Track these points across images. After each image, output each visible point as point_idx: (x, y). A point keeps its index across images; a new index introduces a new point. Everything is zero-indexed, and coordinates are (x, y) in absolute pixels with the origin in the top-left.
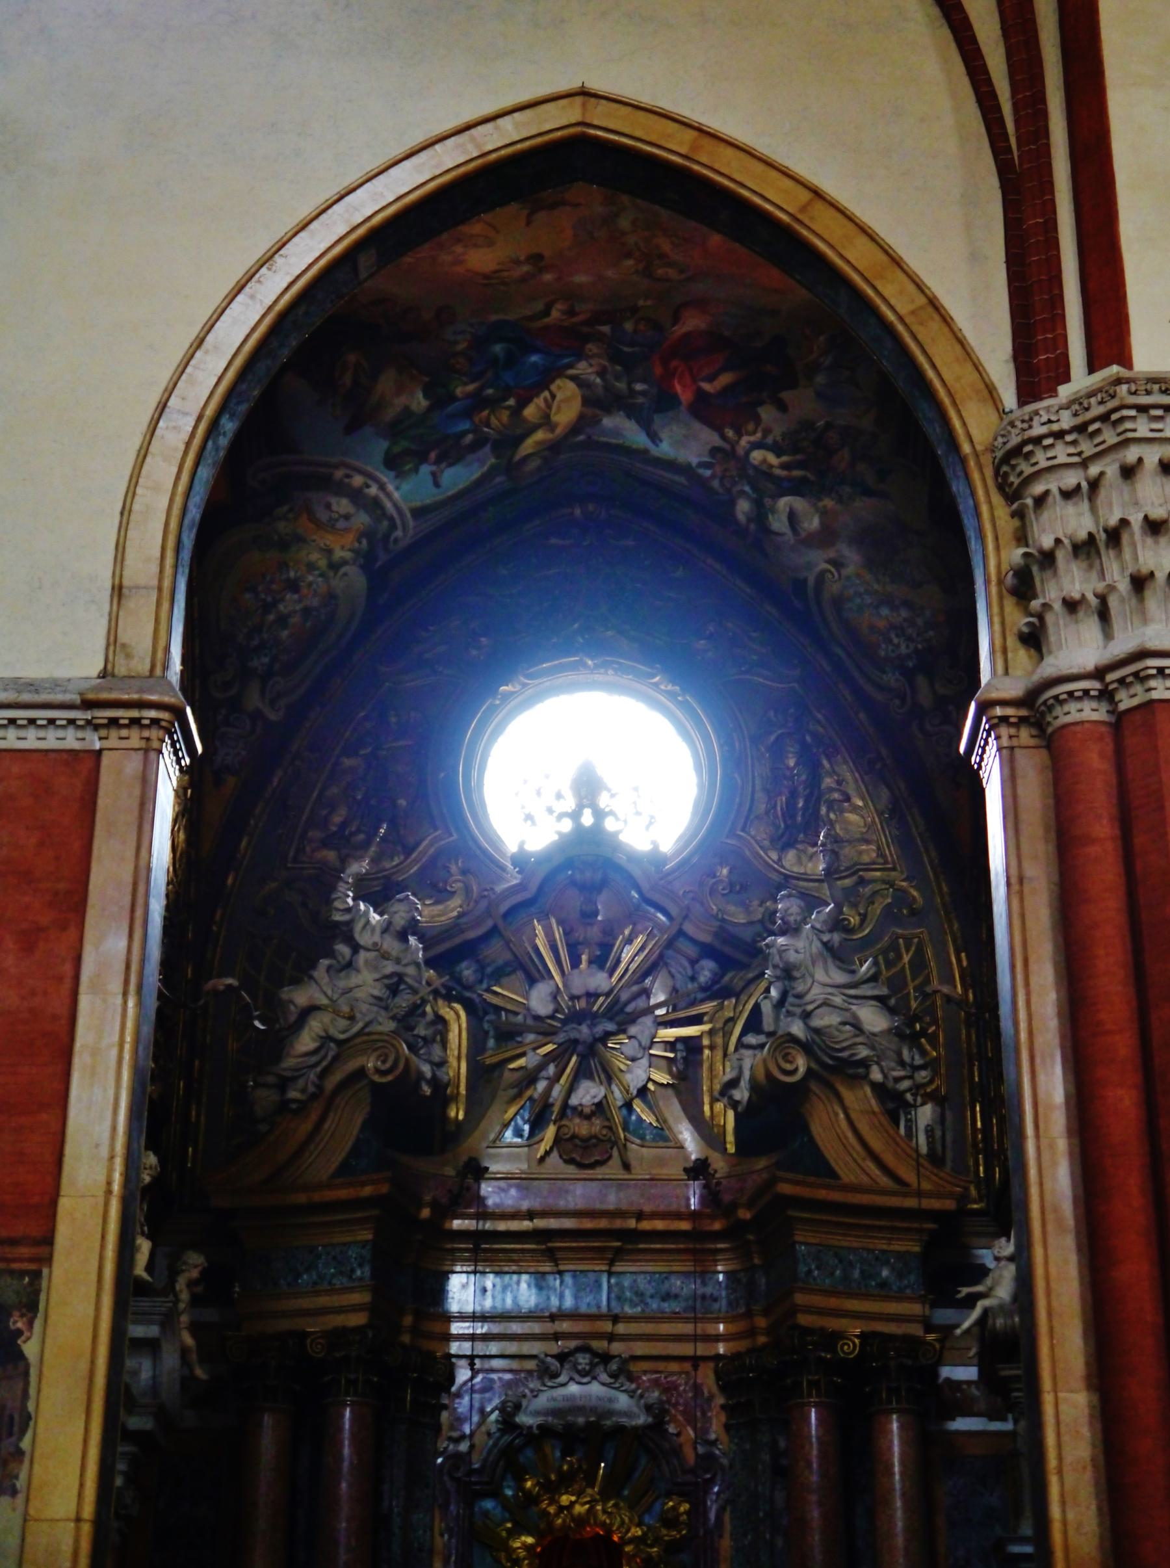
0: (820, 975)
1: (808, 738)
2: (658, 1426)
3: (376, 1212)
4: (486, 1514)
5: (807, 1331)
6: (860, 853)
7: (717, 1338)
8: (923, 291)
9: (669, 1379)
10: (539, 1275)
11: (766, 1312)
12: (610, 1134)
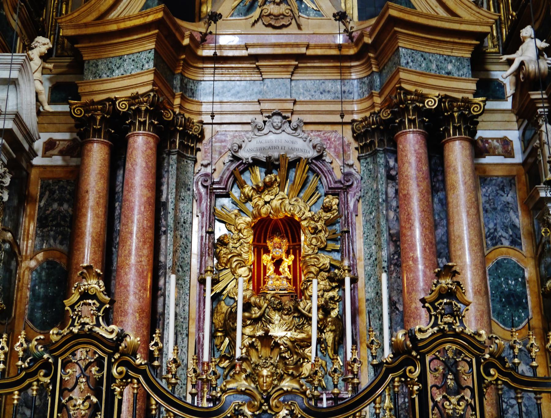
2: (319, 158)
3: (157, 31)
4: (223, 207)
5: (407, 92)
7: (352, 112)
9: (325, 135)
10: (252, 82)
11: (380, 95)
12: (290, 13)
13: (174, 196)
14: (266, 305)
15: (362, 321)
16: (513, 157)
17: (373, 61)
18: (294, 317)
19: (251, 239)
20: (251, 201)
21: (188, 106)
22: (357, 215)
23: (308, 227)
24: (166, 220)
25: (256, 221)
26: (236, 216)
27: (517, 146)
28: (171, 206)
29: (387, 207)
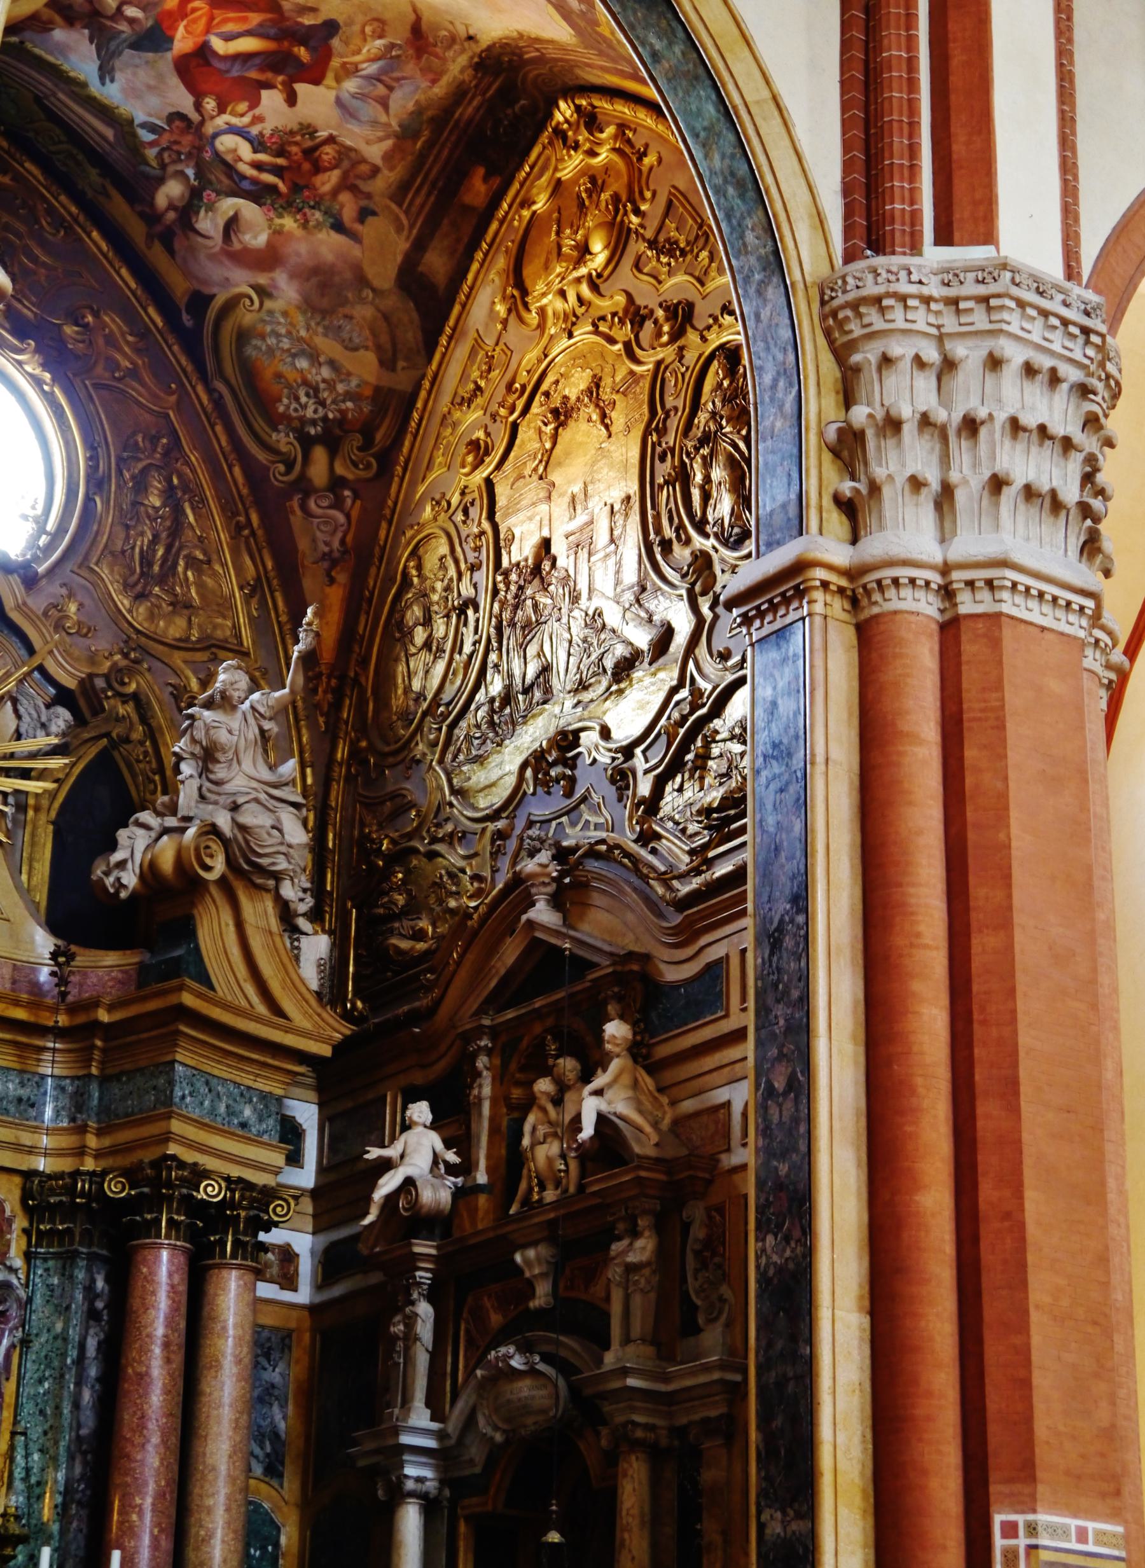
0: (247, 765)
1: (175, 481)
6: (215, 627)
7: (31, 1150)
8: (768, 82)
16: (295, 1290)
17: (97, 1055)
27: (305, 1267)
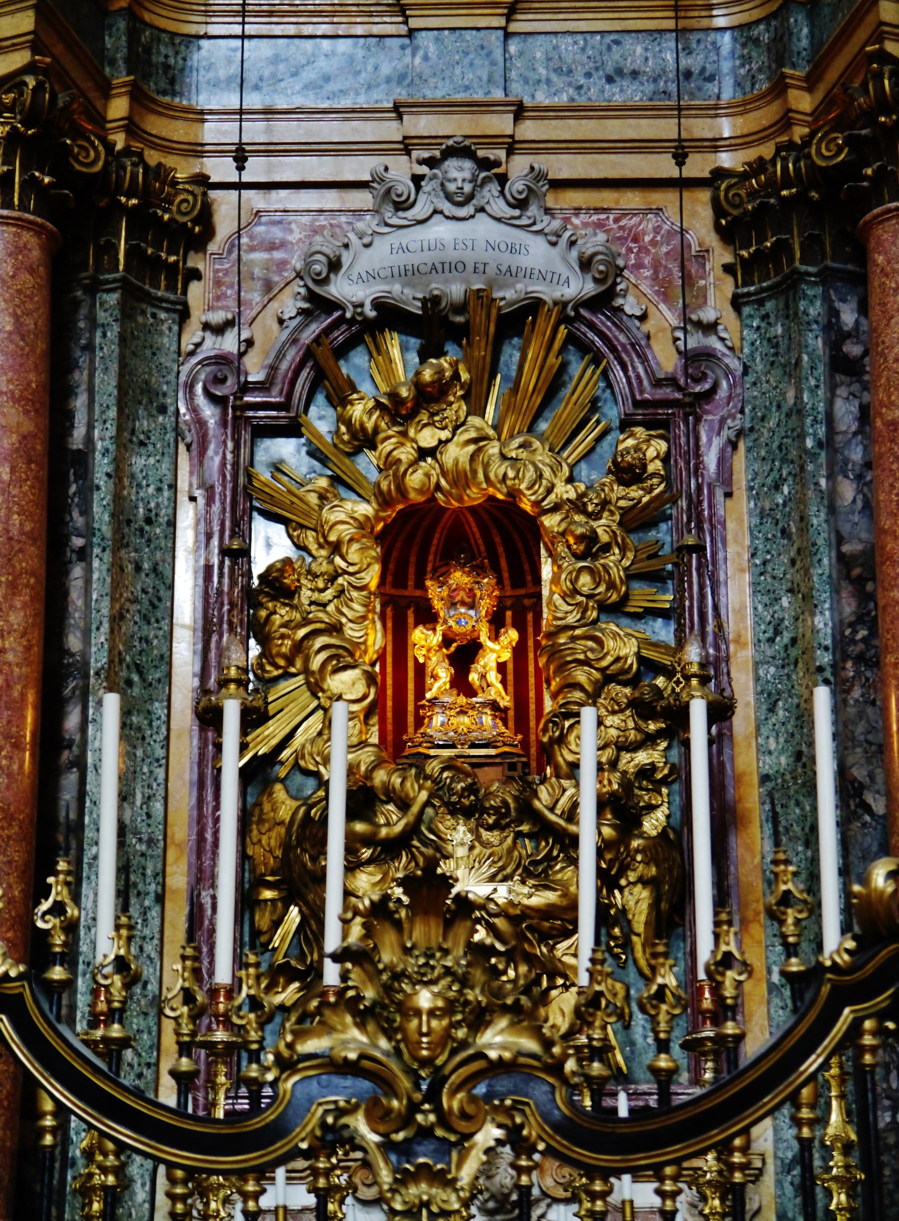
4: (277, 468)
7: (714, 145)
9: (622, 223)
10: (374, 40)
11: (810, 84)
13: (112, 431)
14: (424, 796)
15: (750, 849)
18: (519, 835)
19: (372, 577)
20: (373, 447)
21: (157, 126)
22: (728, 495)
23: (563, 534)
24: (86, 511)
25: (390, 514)
26: (322, 497)
28: (102, 466)
29: (831, 464)
